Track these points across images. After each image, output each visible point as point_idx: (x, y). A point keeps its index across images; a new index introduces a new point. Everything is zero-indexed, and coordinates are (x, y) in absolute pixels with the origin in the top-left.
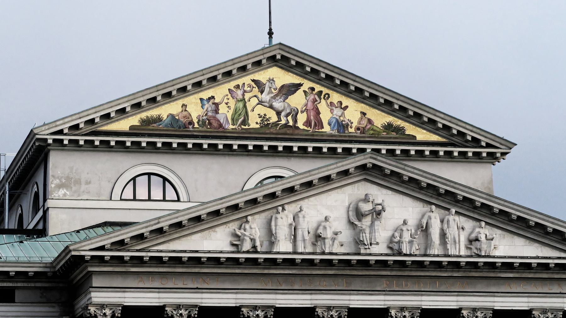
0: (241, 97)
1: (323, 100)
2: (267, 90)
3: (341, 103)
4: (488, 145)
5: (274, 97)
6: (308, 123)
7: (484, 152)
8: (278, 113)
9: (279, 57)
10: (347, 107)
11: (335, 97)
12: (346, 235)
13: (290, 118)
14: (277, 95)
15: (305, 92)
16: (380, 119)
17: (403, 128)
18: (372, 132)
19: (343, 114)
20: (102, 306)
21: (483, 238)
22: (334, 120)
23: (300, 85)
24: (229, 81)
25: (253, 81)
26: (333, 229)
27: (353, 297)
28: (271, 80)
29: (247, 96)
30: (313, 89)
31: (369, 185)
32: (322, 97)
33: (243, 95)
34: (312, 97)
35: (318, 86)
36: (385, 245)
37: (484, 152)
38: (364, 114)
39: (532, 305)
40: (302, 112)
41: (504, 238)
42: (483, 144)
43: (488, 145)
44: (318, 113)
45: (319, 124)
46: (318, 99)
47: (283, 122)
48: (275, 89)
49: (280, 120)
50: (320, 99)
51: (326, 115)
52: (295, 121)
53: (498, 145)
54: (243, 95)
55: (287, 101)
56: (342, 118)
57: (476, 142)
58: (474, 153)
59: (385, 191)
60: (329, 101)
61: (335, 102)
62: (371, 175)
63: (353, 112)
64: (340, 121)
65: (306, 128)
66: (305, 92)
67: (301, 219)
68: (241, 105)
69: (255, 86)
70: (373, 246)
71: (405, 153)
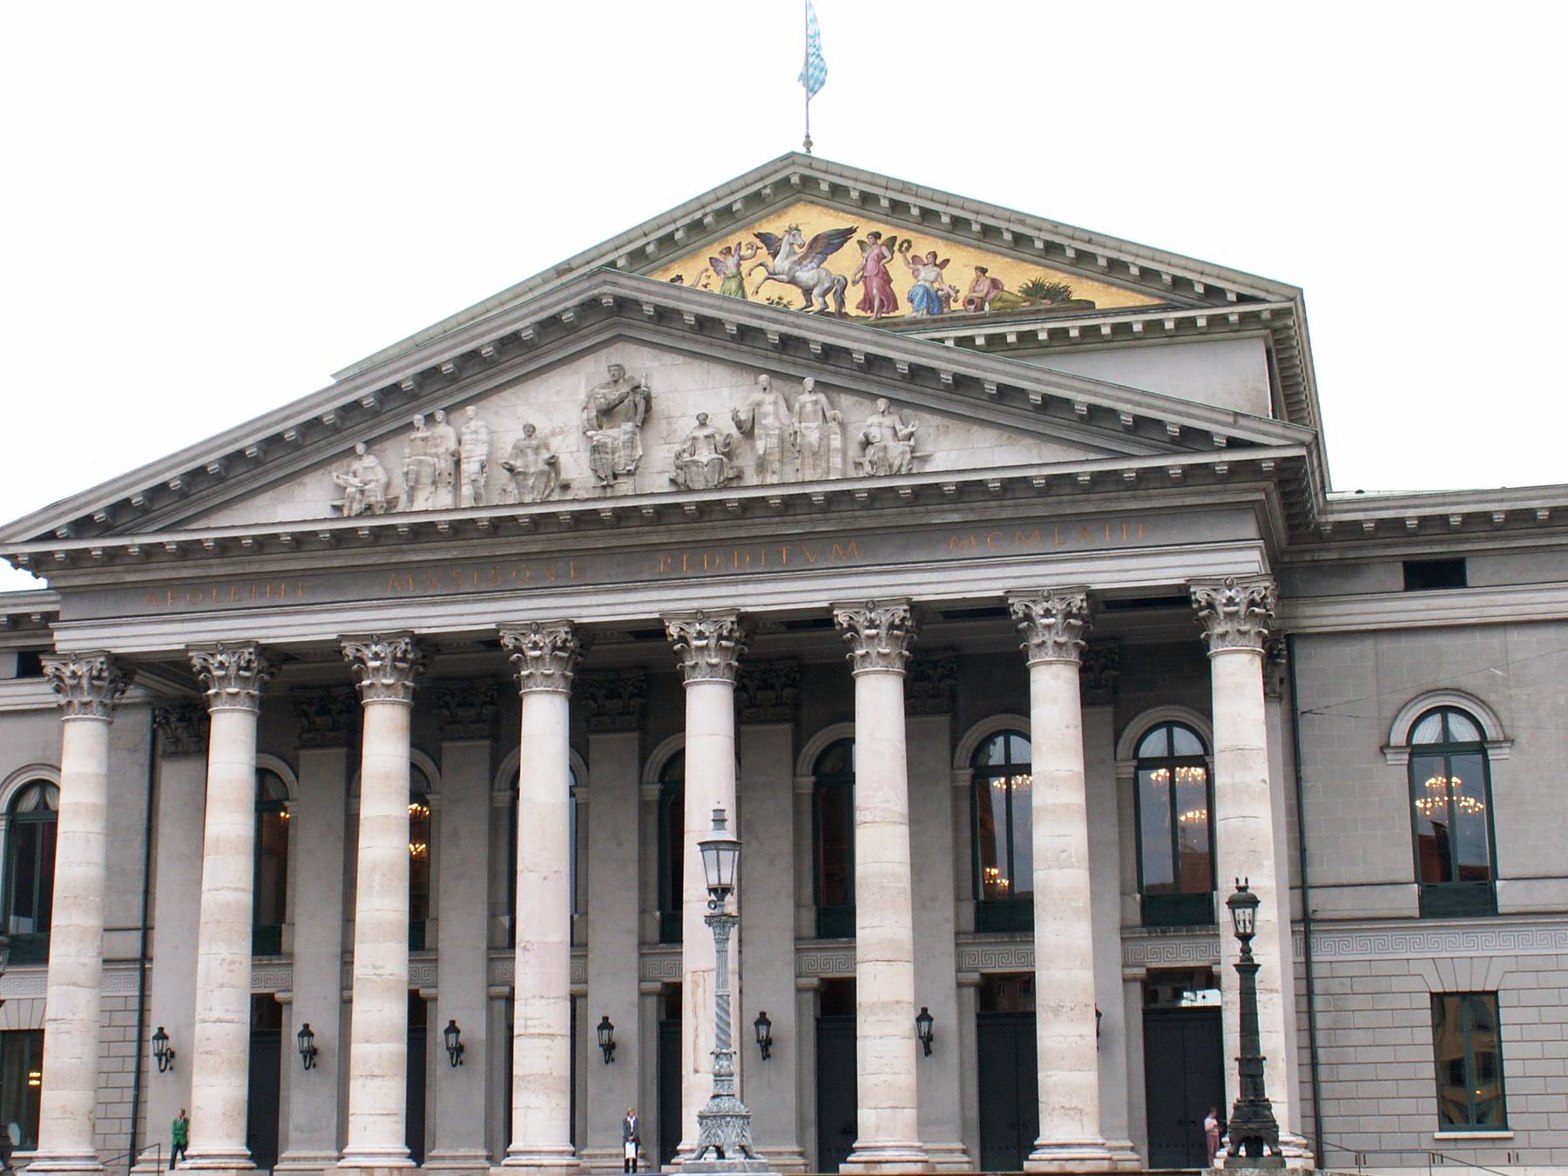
0: (734, 270)
1: (897, 254)
2: (784, 249)
3: (935, 256)
4: (1242, 299)
5: (799, 262)
6: (867, 303)
7: (1234, 312)
8: (807, 292)
9: (795, 180)
10: (947, 261)
11: (923, 246)
12: (577, 468)
13: (830, 298)
14: (804, 257)
15: (861, 243)
16: (1016, 276)
17: (1066, 288)
18: (999, 304)
19: (939, 275)
20: (77, 657)
21: (875, 433)
22: (921, 291)
23: (852, 231)
24: (711, 243)
25: (758, 236)
26: (546, 455)
27: (586, 600)
28: (794, 230)
29: (746, 266)
30: (877, 236)
31: (632, 348)
32: (896, 248)
33: (738, 265)
34: (876, 251)
35: (889, 227)
36: (665, 478)
37: (1234, 312)
38: (984, 271)
39: (1011, 584)
40: (855, 283)
41: (947, 433)
42: (1231, 297)
43: (1242, 299)
44: (887, 280)
45: (890, 301)
46: (887, 253)
47: (817, 306)
48: (801, 246)
49: (810, 303)
50: (892, 253)
51: (903, 281)
52: (841, 303)
53: (1262, 295)
54: (738, 265)
55: (824, 265)
56: (936, 285)
57: (1213, 294)
58: (1211, 320)
59: (668, 358)
60: (909, 256)
61: (923, 255)
62: (630, 326)
63: (961, 271)
64: (932, 291)
65: (863, 314)
66: (861, 243)
67: (466, 438)
68: (733, 285)
69: (760, 244)
70: (621, 480)
71: (1058, 335)
